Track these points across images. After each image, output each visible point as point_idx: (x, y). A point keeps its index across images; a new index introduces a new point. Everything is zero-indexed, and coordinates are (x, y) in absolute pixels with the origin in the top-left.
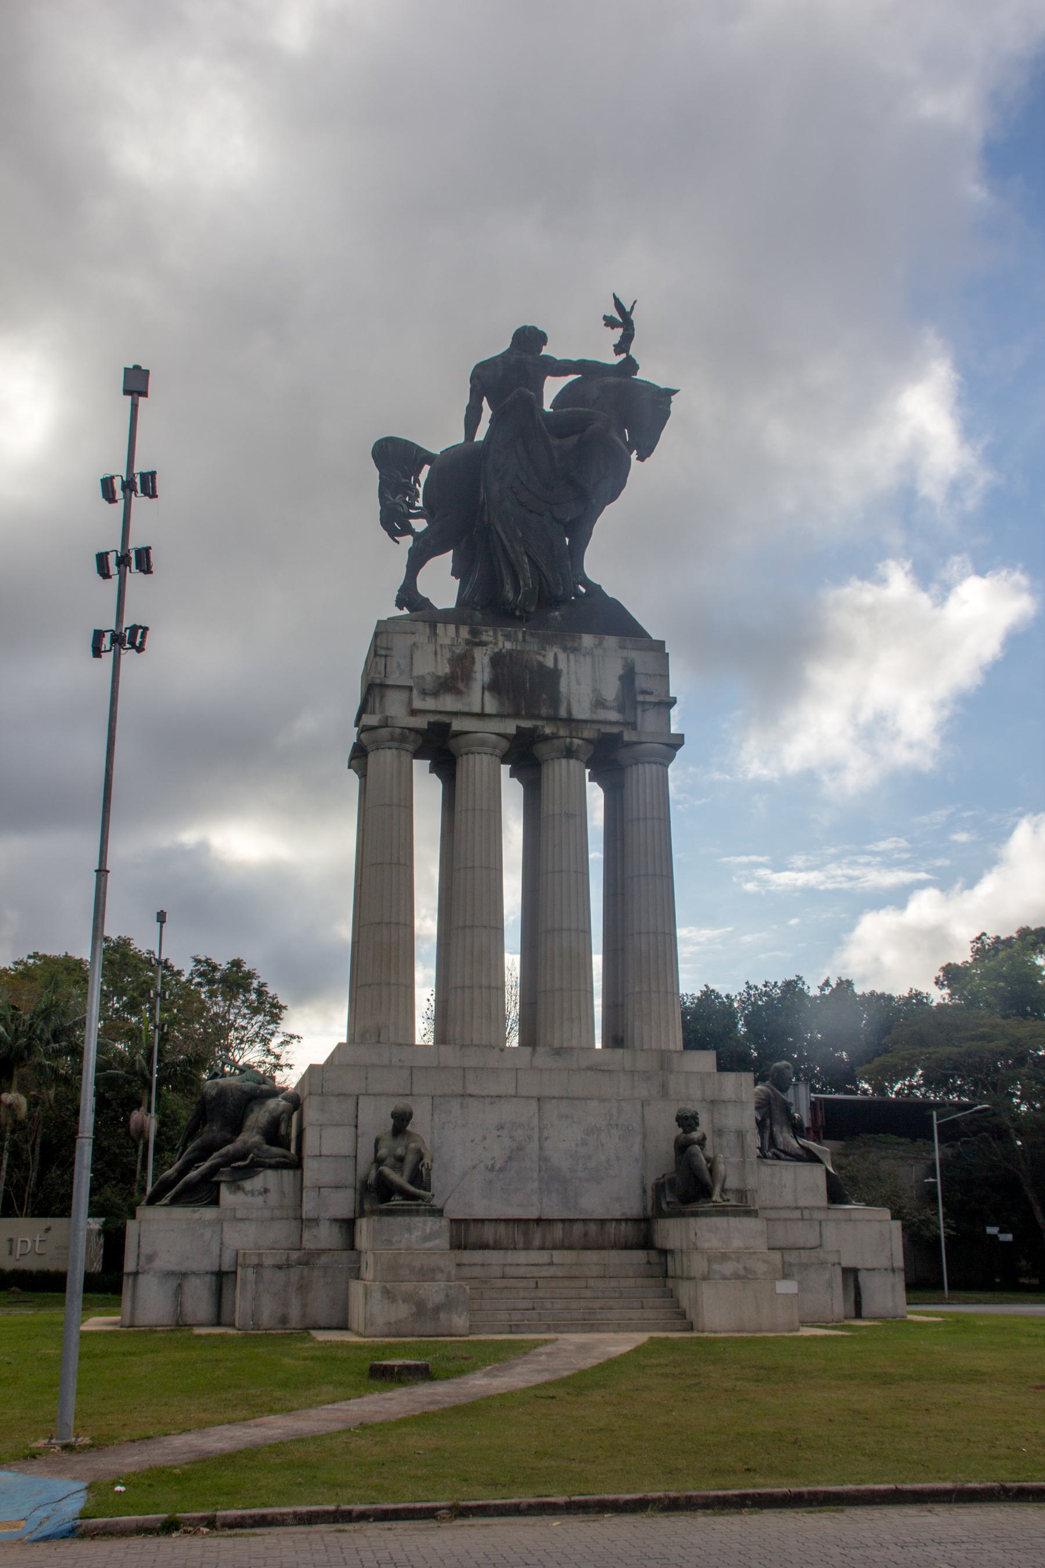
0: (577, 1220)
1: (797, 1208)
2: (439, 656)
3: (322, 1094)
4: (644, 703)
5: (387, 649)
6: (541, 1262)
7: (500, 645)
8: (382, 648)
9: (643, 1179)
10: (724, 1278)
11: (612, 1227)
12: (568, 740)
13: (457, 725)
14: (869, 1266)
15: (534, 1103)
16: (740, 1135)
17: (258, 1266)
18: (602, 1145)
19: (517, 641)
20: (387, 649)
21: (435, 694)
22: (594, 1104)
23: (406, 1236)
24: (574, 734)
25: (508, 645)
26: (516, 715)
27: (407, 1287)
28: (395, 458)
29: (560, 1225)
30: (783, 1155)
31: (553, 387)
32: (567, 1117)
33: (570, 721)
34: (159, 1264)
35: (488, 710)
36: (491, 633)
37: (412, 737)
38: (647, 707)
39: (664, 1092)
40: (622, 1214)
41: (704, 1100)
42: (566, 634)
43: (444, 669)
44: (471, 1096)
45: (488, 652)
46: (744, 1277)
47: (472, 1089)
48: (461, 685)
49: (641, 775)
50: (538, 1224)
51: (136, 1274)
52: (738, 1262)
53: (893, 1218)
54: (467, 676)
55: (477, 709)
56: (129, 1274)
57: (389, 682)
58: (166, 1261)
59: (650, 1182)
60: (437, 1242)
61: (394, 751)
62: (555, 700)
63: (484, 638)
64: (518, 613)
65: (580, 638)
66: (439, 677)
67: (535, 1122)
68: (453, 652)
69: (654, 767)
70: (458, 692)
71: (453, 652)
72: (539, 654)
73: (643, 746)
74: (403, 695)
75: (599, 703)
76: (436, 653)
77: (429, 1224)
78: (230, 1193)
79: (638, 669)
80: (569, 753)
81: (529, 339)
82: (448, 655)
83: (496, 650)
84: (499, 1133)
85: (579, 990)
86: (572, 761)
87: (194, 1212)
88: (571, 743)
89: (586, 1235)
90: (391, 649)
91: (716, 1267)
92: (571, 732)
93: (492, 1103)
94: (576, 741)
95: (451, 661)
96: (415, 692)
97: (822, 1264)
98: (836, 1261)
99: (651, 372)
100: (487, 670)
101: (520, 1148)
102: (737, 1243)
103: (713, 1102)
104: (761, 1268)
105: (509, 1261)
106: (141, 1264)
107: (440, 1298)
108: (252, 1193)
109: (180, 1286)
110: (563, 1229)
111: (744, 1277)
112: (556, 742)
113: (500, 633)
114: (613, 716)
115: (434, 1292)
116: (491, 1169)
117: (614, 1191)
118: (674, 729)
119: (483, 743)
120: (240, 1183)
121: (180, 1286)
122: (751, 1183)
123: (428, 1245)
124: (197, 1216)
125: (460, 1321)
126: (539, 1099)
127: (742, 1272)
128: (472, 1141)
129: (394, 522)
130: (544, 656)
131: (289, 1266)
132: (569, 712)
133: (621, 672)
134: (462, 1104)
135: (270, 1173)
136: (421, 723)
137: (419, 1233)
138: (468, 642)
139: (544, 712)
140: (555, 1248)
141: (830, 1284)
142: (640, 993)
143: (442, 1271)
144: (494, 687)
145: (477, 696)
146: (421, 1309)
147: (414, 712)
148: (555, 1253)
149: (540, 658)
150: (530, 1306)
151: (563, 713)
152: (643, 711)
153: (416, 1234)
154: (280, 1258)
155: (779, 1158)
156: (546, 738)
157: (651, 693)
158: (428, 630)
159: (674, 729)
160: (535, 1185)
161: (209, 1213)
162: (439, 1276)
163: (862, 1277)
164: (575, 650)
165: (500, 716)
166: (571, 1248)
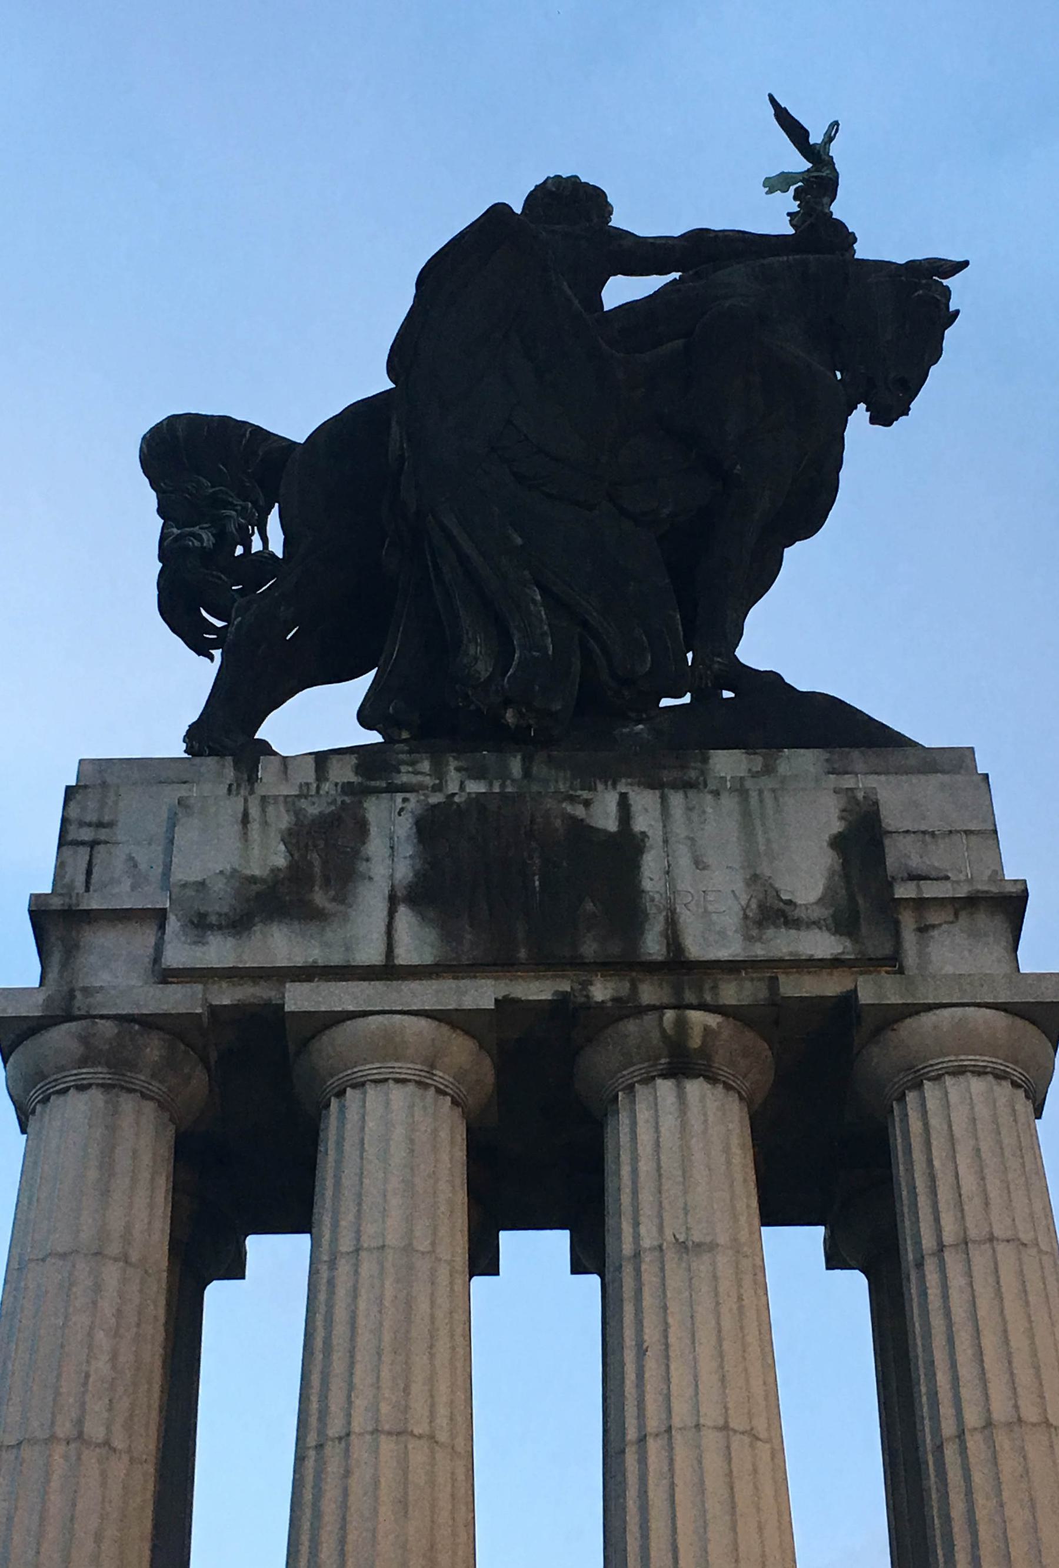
2: (255, 827)
4: (920, 904)
5: (100, 825)
7: (453, 787)
8: (82, 824)
12: (669, 1015)
13: (298, 998)
20: (100, 825)
24: (690, 997)
25: (475, 787)
26: (500, 964)
33: (678, 966)
35: (407, 954)
36: (425, 766)
37: (153, 1049)
38: (933, 917)
43: (271, 856)
45: (411, 805)
48: (320, 898)
55: (371, 954)
57: (94, 903)
61: (96, 1096)
62: (626, 907)
64: (510, 716)
65: (705, 760)
66: (253, 880)
68: (298, 813)
69: (977, 1085)
71: (298, 813)
72: (572, 799)
73: (928, 1019)
74: (140, 941)
75: (772, 912)
76: (245, 819)
79: (892, 818)
80: (682, 1063)
82: (283, 820)
83: (436, 799)
86: (694, 1088)
88: (681, 1024)
92: (678, 991)
94: (696, 1016)
95: (293, 838)
96: (173, 924)
99: (881, 228)
100: (406, 849)
112: (631, 1027)
114: (822, 945)
119: (390, 1048)
130: (587, 804)
133: (837, 827)
136: (178, 1000)
139: (589, 949)
145: (370, 923)
147: (166, 976)
151: (653, 946)
152: (923, 930)
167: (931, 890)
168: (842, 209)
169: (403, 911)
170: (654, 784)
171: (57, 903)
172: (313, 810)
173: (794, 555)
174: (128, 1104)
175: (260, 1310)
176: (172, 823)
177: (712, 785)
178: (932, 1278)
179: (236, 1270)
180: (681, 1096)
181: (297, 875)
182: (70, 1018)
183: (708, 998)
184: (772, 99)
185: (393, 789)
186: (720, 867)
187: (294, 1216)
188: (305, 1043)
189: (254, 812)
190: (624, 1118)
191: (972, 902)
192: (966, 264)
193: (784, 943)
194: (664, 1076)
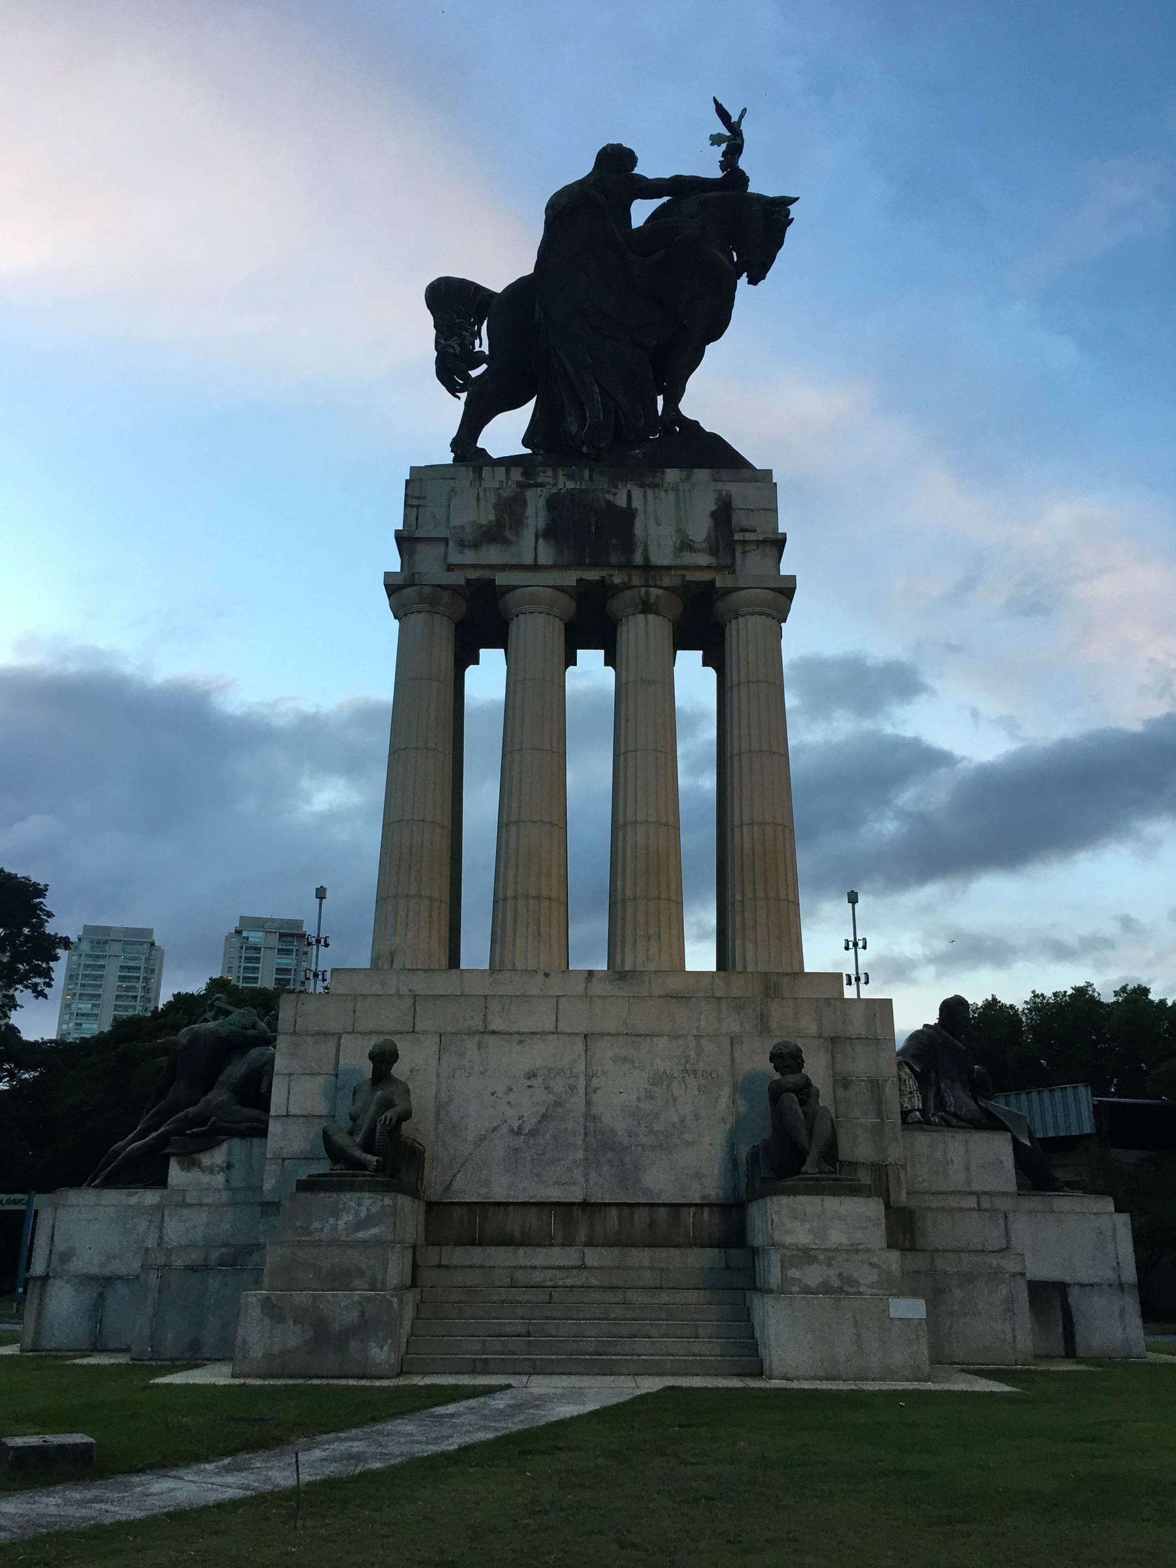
0: (638, 1205)
1: (971, 1193)
2: (482, 503)
3: (295, 1033)
4: (744, 542)
5: (419, 498)
6: (567, 1263)
7: (561, 486)
8: (412, 497)
9: (732, 1146)
10: (807, 1290)
11: (689, 1216)
12: (643, 590)
13: (501, 579)
14: (1085, 1279)
15: (579, 1042)
16: (875, 1085)
17: (165, 1268)
18: (675, 1099)
19: (581, 480)
20: (419, 498)
21: (476, 545)
22: (663, 1042)
23: (332, 1221)
24: (651, 583)
25: (570, 485)
26: (579, 564)
27: (301, 1297)
28: (452, 301)
29: (614, 1212)
30: (954, 1121)
31: (641, 211)
32: (625, 1059)
33: (647, 567)
34: (78, 1265)
35: (542, 561)
36: (550, 473)
37: (446, 597)
39: (763, 1025)
40: (703, 1197)
41: (820, 1037)
42: (647, 472)
43: (488, 516)
44: (493, 1032)
45: (544, 494)
46: (838, 1291)
47: (496, 1024)
48: (508, 534)
49: (742, 633)
50: (583, 1211)
51: (45, 1278)
52: (829, 1265)
53: (1117, 1210)
54: (518, 523)
55: (528, 560)
56: (36, 1278)
58: (87, 1262)
59: (744, 1152)
60: (376, 1230)
62: (628, 542)
63: (541, 479)
64: (584, 449)
65: (663, 473)
66: (481, 526)
67: (580, 1067)
68: (499, 496)
70: (506, 542)
71: (499, 496)
72: (609, 492)
73: (744, 592)
74: (439, 549)
75: (686, 545)
76: (478, 499)
77: (367, 1202)
78: (182, 1169)
79: (737, 503)
80: (647, 607)
81: (615, 162)
82: (493, 499)
83: (554, 491)
84: (532, 1082)
85: (659, 898)
86: (651, 617)
87: (130, 1195)
88: (647, 594)
89: (659, 1225)
90: (425, 498)
91: (793, 1273)
92: (646, 580)
93: (521, 1042)
94: (654, 591)
96: (451, 543)
97: (996, 1275)
98: (1018, 1269)
100: (542, 513)
101: (558, 1104)
102: (837, 1237)
103: (833, 1040)
104: (866, 1276)
105: (522, 1262)
106: (52, 1266)
107: (353, 1316)
108: (211, 1170)
109: (101, 1296)
110: (620, 1218)
111: (840, 1290)
112: (628, 593)
113: (561, 473)
114: (704, 559)
115: (342, 1306)
116: (518, 1132)
117: (690, 1165)
118: (785, 569)
120: (196, 1156)
121: (101, 1296)
122: (895, 1153)
123: (361, 1235)
124: (133, 1200)
125: (381, 1354)
126: (586, 1036)
127: (835, 1283)
128: (493, 1094)
129: (450, 370)
130: (614, 494)
131: (207, 1267)
132: (646, 557)
133: (713, 507)
134: (480, 1046)
135: (236, 1142)
136: (457, 578)
137: (351, 1218)
138: (520, 485)
139: (613, 559)
140: (608, 1244)
141: (1009, 1305)
142: (742, 901)
143: (361, 1273)
144: (550, 533)
145: (529, 545)
146: (321, 1331)
147: (450, 568)
148: (588, 1251)
149: (610, 498)
150: (524, 1331)
151: (638, 559)
152: (744, 553)
153: (347, 1218)
154: (194, 1257)
155: (949, 1125)
156: (615, 590)
157: (755, 531)
158: (471, 475)
159: (785, 569)
160: (580, 1155)
161: (150, 1197)
162: (357, 1283)
163: (1074, 1295)
164: (655, 486)
165: (554, 567)
166: (631, 1244)
167: (749, 536)
168: (743, 163)
169: (541, 541)
170: (642, 486)
171: (405, 534)
172: (505, 495)
173: (710, 348)
174: (438, 617)
175: (487, 679)
176: (450, 498)
177: (665, 486)
178: (735, 694)
179: (476, 661)
180: (646, 619)
181: (499, 524)
182: (411, 586)
183: (658, 583)
184: (715, 100)
185: (537, 485)
186: (668, 520)
187: (498, 640)
188: (503, 594)
189: (482, 494)
190: (624, 628)
191: (765, 542)
192: (797, 199)
193: (689, 558)
194: (641, 613)
